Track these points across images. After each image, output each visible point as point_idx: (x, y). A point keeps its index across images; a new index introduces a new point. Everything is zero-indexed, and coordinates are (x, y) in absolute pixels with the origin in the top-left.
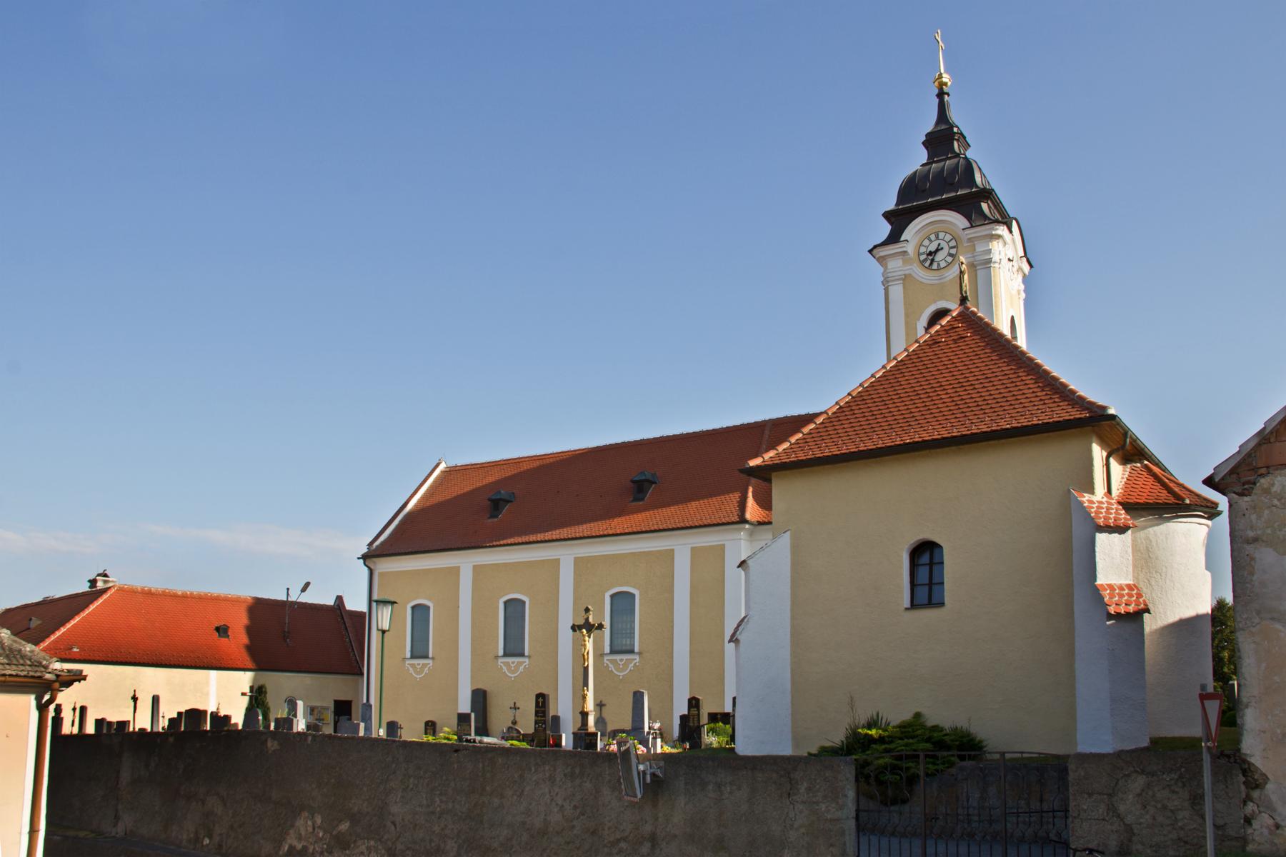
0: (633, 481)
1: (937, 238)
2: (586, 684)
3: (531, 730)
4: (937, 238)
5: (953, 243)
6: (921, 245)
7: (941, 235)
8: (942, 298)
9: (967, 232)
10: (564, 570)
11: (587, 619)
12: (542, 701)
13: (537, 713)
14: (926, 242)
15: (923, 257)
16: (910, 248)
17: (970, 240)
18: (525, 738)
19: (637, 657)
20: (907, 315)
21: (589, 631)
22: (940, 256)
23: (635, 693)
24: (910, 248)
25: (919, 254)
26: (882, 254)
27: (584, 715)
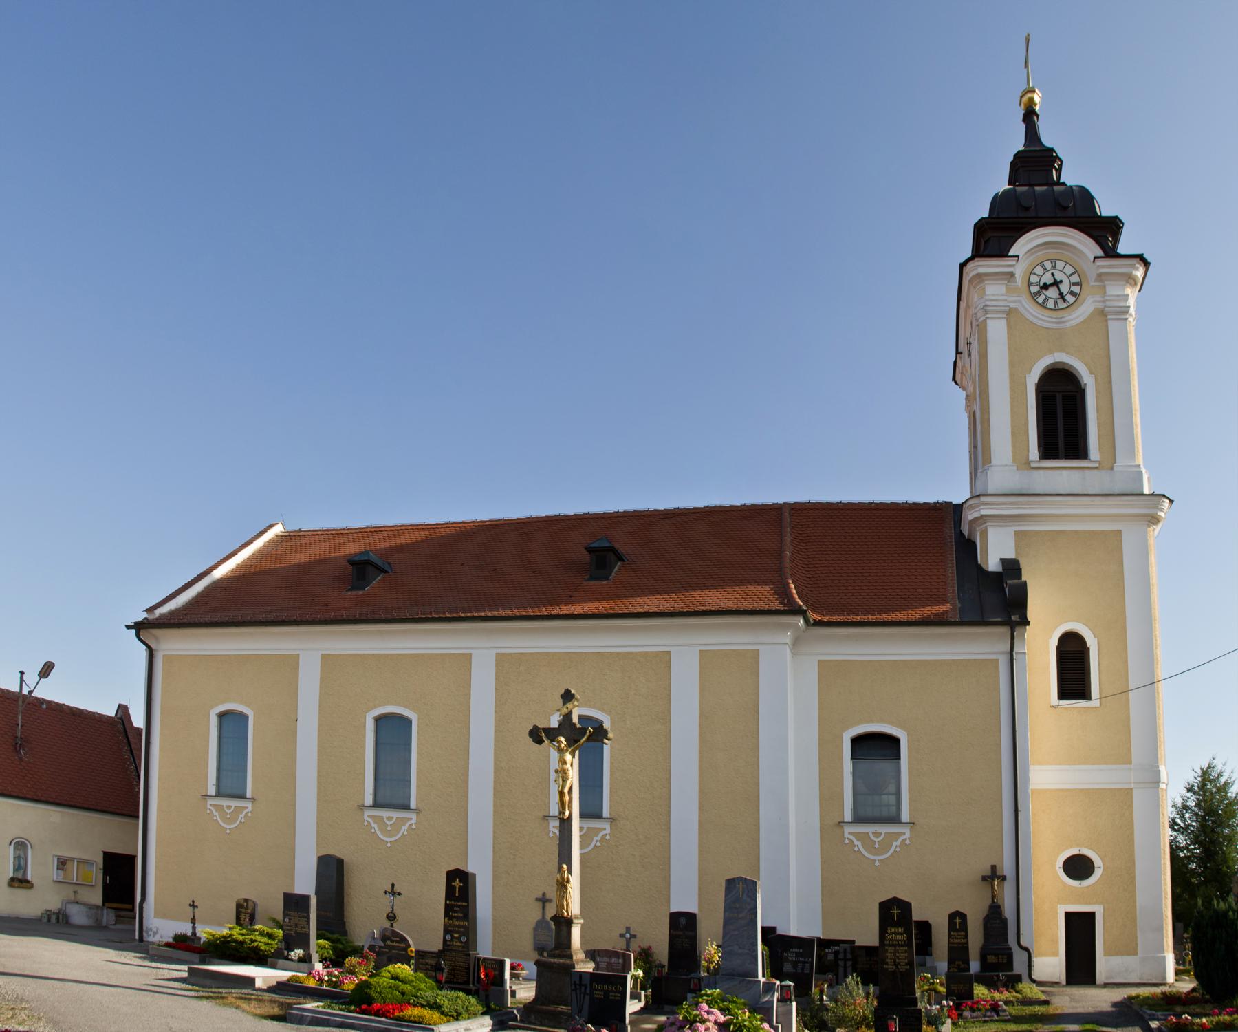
0: (590, 550)
1: (1054, 267)
2: (565, 855)
3: (435, 943)
4: (1054, 267)
5: (1075, 279)
6: (1032, 272)
7: (1060, 265)
8: (1062, 350)
9: (1099, 262)
10: (479, 678)
11: (568, 716)
12: (459, 888)
13: (448, 910)
14: (1039, 270)
15: (1035, 289)
16: (1019, 270)
17: (1100, 277)
18: (423, 961)
19: (607, 826)
20: (1012, 364)
21: (572, 742)
22: (1052, 293)
23: (731, 883)
24: (1019, 270)
25: (1029, 285)
26: (981, 270)
27: (564, 923)
